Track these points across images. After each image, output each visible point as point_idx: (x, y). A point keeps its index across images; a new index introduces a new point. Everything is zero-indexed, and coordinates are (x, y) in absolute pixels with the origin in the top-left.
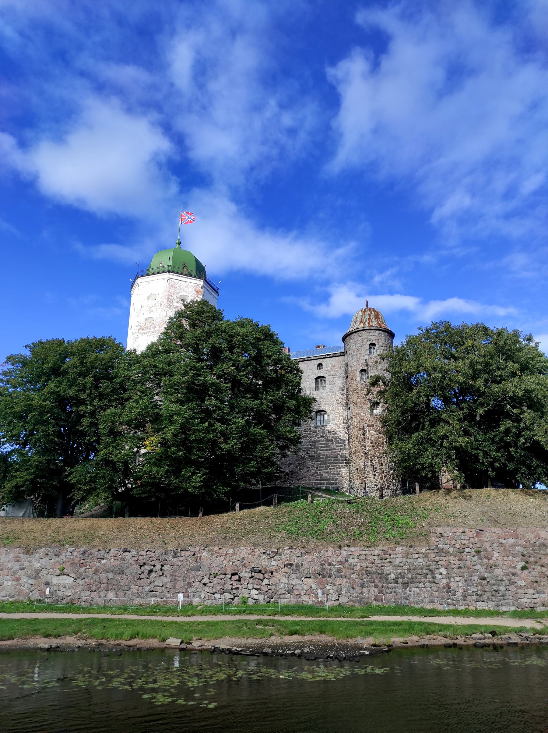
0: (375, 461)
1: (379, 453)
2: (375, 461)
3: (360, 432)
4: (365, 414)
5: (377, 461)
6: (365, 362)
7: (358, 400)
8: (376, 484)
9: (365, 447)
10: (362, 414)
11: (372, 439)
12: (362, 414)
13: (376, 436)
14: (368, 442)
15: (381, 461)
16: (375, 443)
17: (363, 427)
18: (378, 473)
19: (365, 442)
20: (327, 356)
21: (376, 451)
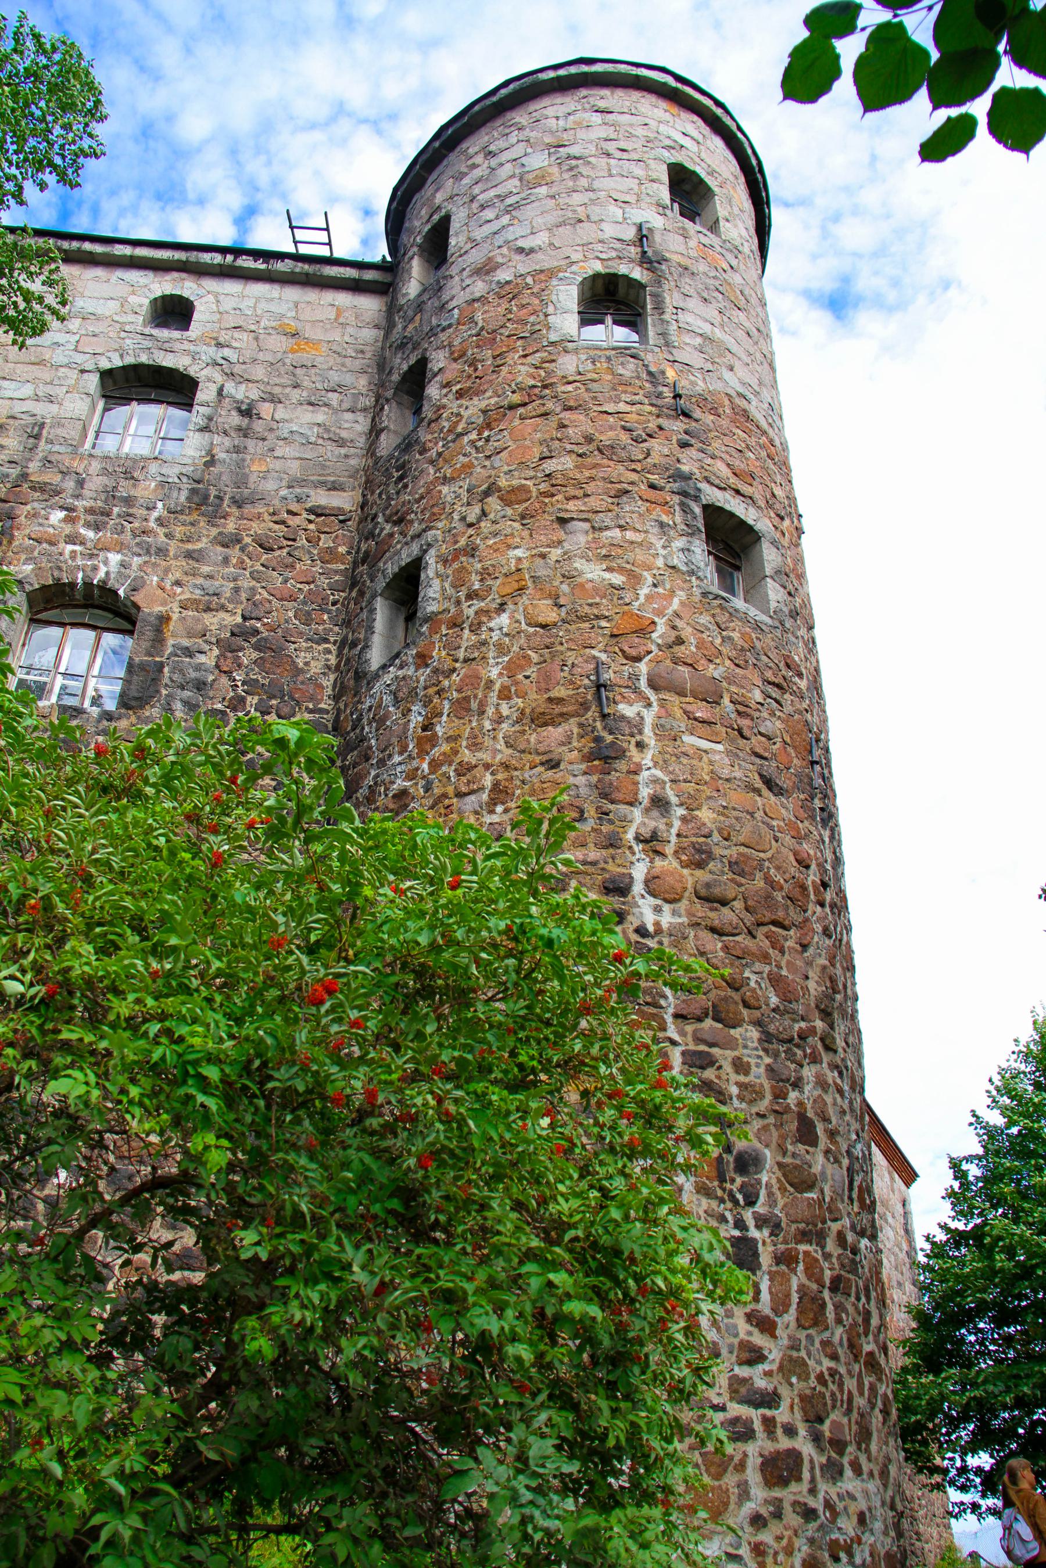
0: (740, 1066)
1: (775, 981)
2: (740, 1066)
3: (554, 733)
4: (634, 579)
5: (758, 1075)
6: (630, 234)
7: (550, 466)
8: (758, 1377)
9: (618, 888)
10: (593, 572)
11: (706, 815)
12: (593, 572)
13: (737, 797)
14: (651, 842)
15: (797, 1085)
16: (737, 867)
17: (599, 686)
18: (776, 1228)
19: (613, 843)
20: (246, 263)
21: (739, 957)
